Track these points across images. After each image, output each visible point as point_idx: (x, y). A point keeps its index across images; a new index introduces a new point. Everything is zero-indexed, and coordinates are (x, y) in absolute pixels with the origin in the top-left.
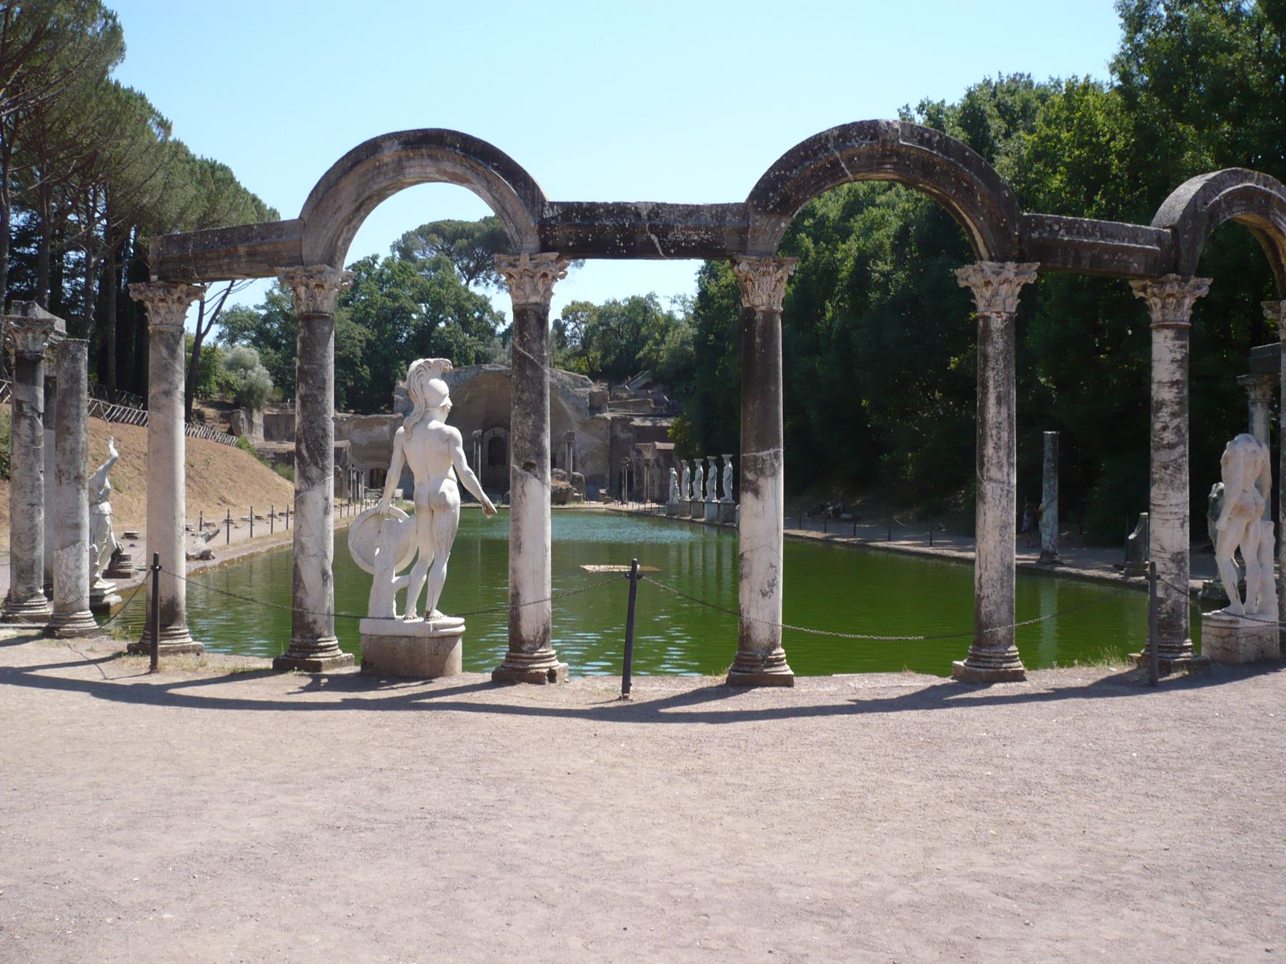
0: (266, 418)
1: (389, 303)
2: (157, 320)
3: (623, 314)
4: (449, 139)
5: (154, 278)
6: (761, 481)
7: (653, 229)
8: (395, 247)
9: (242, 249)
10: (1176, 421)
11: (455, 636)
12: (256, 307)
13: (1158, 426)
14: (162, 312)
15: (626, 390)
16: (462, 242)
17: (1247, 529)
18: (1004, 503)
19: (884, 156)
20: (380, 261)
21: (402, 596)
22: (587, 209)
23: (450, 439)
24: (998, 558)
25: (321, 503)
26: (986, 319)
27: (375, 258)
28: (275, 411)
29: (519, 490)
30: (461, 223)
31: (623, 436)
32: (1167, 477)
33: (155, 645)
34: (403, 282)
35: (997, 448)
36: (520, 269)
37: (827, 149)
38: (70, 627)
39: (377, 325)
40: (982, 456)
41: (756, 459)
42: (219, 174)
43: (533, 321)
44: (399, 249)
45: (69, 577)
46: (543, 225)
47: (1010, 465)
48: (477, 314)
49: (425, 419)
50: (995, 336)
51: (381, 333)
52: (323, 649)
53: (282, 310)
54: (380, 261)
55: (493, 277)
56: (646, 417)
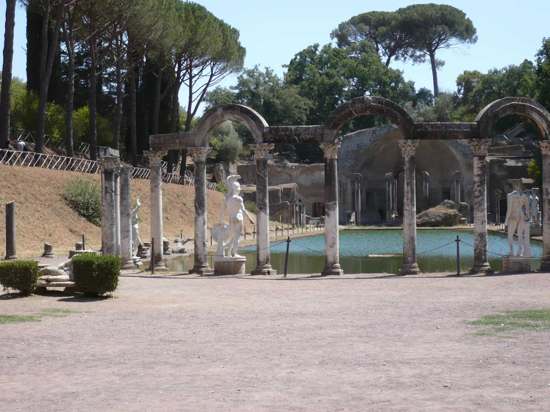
0: (239, 168)
1: (326, 81)
2: (152, 163)
3: (502, 81)
4: (236, 108)
5: (151, 149)
6: (330, 212)
7: (296, 135)
8: (334, 34)
9: (177, 141)
10: (479, 188)
11: (242, 262)
12: (231, 88)
14: (154, 160)
15: (505, 141)
16: (382, 29)
17: (518, 225)
18: (410, 217)
19: (366, 108)
20: (320, 49)
21: (226, 251)
23: (239, 201)
25: (202, 221)
27: (316, 47)
28: (246, 163)
30: (382, 13)
31: (500, 174)
33: (153, 268)
34: (337, 63)
35: (407, 199)
36: (257, 148)
37: (348, 108)
38: (126, 266)
39: (320, 97)
41: (328, 205)
42: (198, 13)
44: (337, 36)
45: (125, 249)
46: (264, 134)
48: (393, 84)
49: (232, 194)
50: (406, 163)
51: (321, 104)
52: (204, 267)
53: (249, 90)
54: (320, 49)
55: (410, 53)
56: (517, 159)
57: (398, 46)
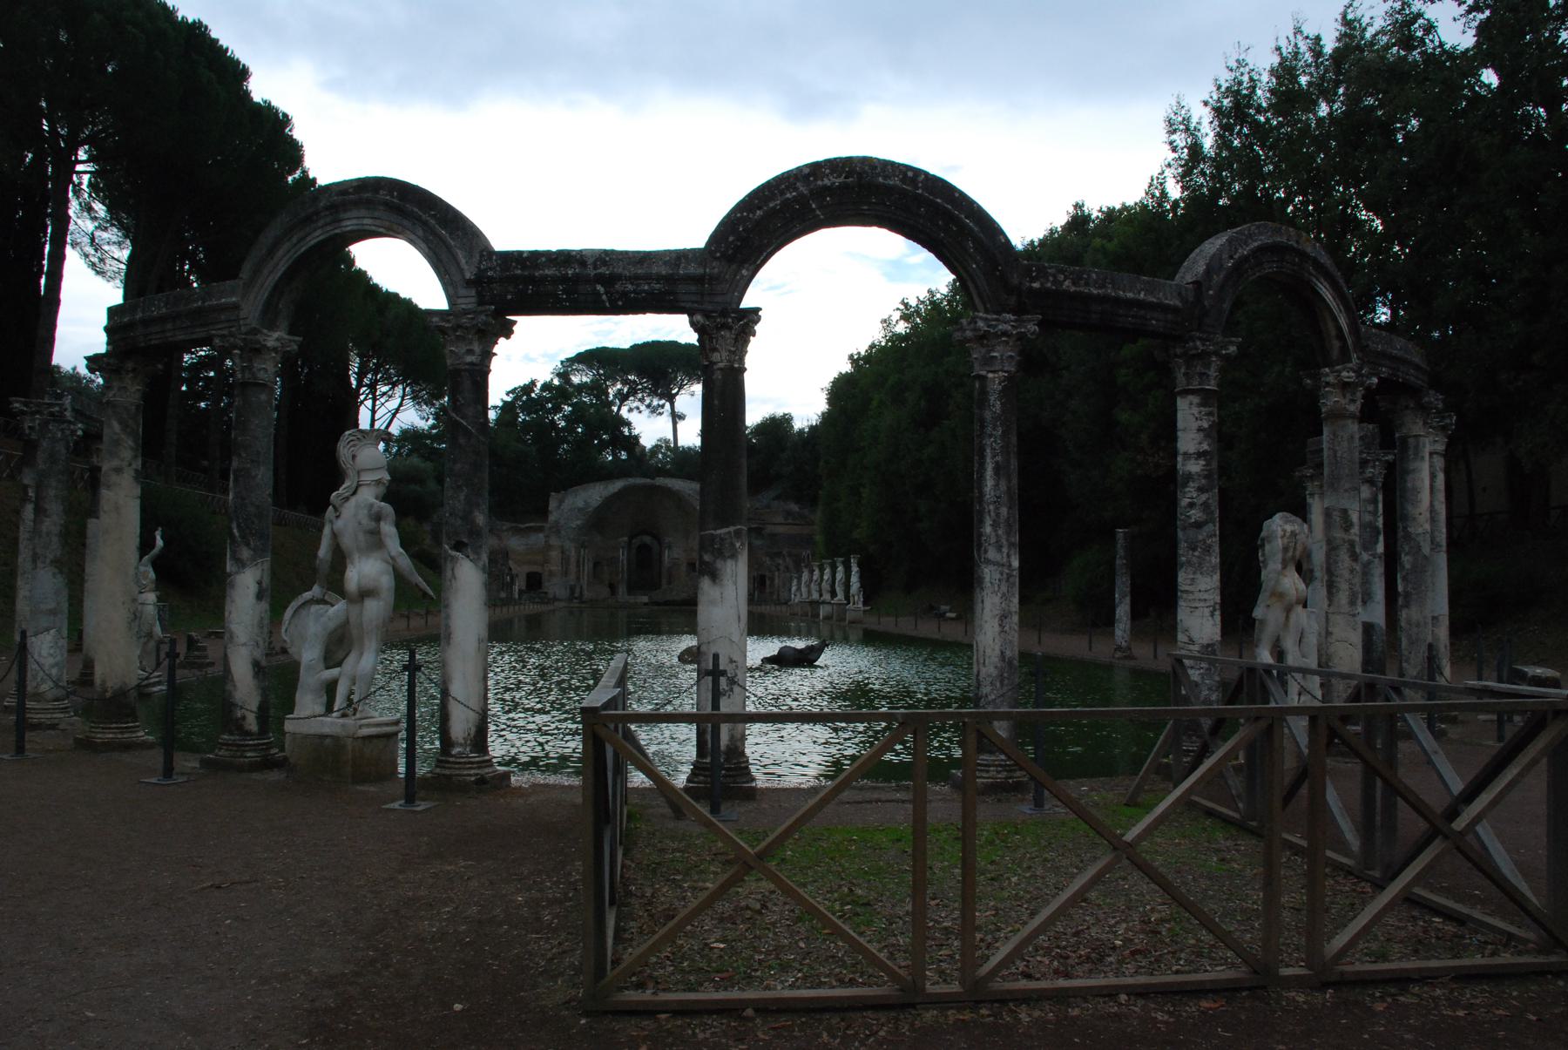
6: (719, 564)
10: (1204, 497)
13: (1185, 502)
18: (1004, 588)
22: (527, 259)
24: (997, 652)
26: (983, 378)
27: (533, 383)
29: (449, 574)
32: (1195, 560)
35: (995, 525)
40: (980, 535)
43: (467, 384)
44: (559, 375)
47: (1011, 545)
54: (539, 385)
57: (633, 392)
